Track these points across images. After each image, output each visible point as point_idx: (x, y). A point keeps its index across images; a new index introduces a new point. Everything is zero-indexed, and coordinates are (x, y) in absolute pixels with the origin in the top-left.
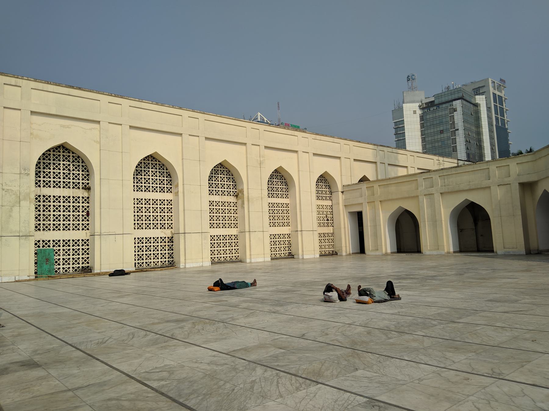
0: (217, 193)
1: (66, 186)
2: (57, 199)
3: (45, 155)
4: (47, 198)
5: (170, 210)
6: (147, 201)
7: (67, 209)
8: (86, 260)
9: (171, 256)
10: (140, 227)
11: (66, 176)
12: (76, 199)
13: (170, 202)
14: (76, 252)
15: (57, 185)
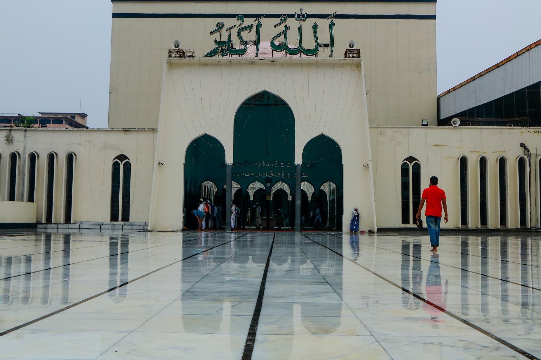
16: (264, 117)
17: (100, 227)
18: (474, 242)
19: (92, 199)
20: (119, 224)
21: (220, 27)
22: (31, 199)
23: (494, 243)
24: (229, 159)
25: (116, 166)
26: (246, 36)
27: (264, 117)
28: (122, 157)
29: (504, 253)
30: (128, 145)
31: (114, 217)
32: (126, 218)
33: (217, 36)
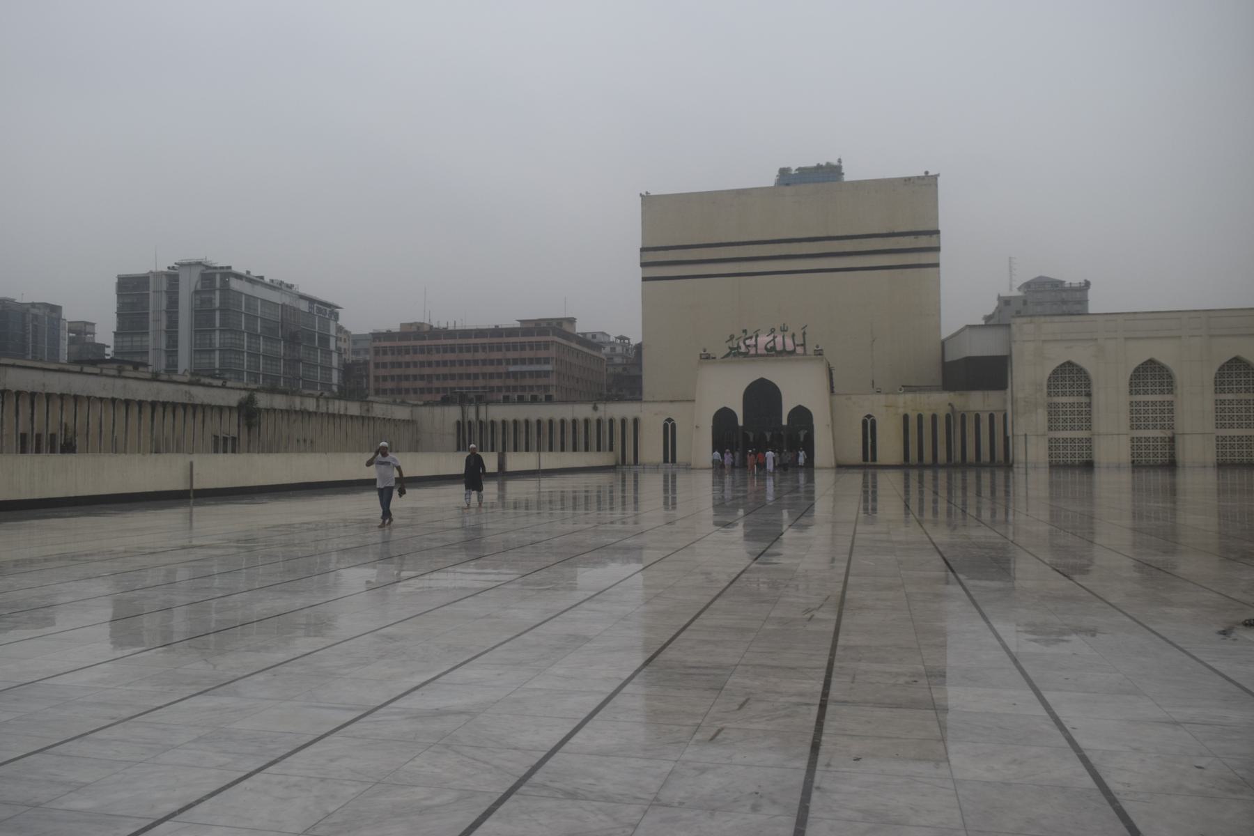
0: (1230, 391)
1: (1072, 394)
2: (1064, 405)
3: (1055, 372)
4: (1057, 405)
5: (1171, 411)
6: (1146, 403)
7: (1072, 413)
8: (1090, 455)
9: (1173, 455)
10: (1138, 428)
11: (1071, 386)
12: (1080, 404)
13: (1171, 403)
14: (1081, 448)
15: (1064, 394)
16: (762, 396)
17: (658, 466)
18: (914, 474)
19: (652, 449)
20: (669, 465)
21: (732, 337)
22: (611, 449)
23: (928, 474)
24: (740, 423)
25: (666, 426)
26: (748, 342)
27: (762, 396)
28: (669, 420)
29: (921, 482)
30: (675, 411)
31: (666, 461)
32: (674, 461)
33: (730, 344)
